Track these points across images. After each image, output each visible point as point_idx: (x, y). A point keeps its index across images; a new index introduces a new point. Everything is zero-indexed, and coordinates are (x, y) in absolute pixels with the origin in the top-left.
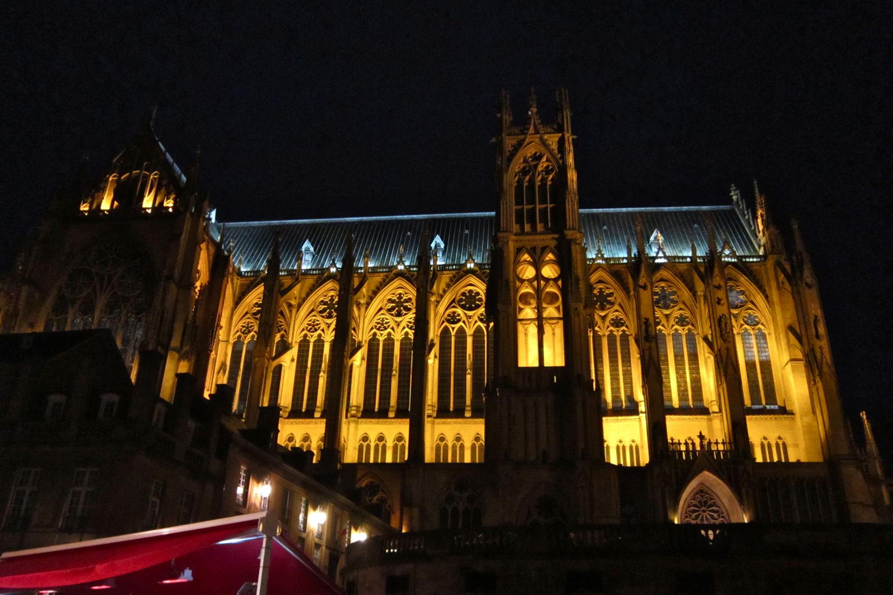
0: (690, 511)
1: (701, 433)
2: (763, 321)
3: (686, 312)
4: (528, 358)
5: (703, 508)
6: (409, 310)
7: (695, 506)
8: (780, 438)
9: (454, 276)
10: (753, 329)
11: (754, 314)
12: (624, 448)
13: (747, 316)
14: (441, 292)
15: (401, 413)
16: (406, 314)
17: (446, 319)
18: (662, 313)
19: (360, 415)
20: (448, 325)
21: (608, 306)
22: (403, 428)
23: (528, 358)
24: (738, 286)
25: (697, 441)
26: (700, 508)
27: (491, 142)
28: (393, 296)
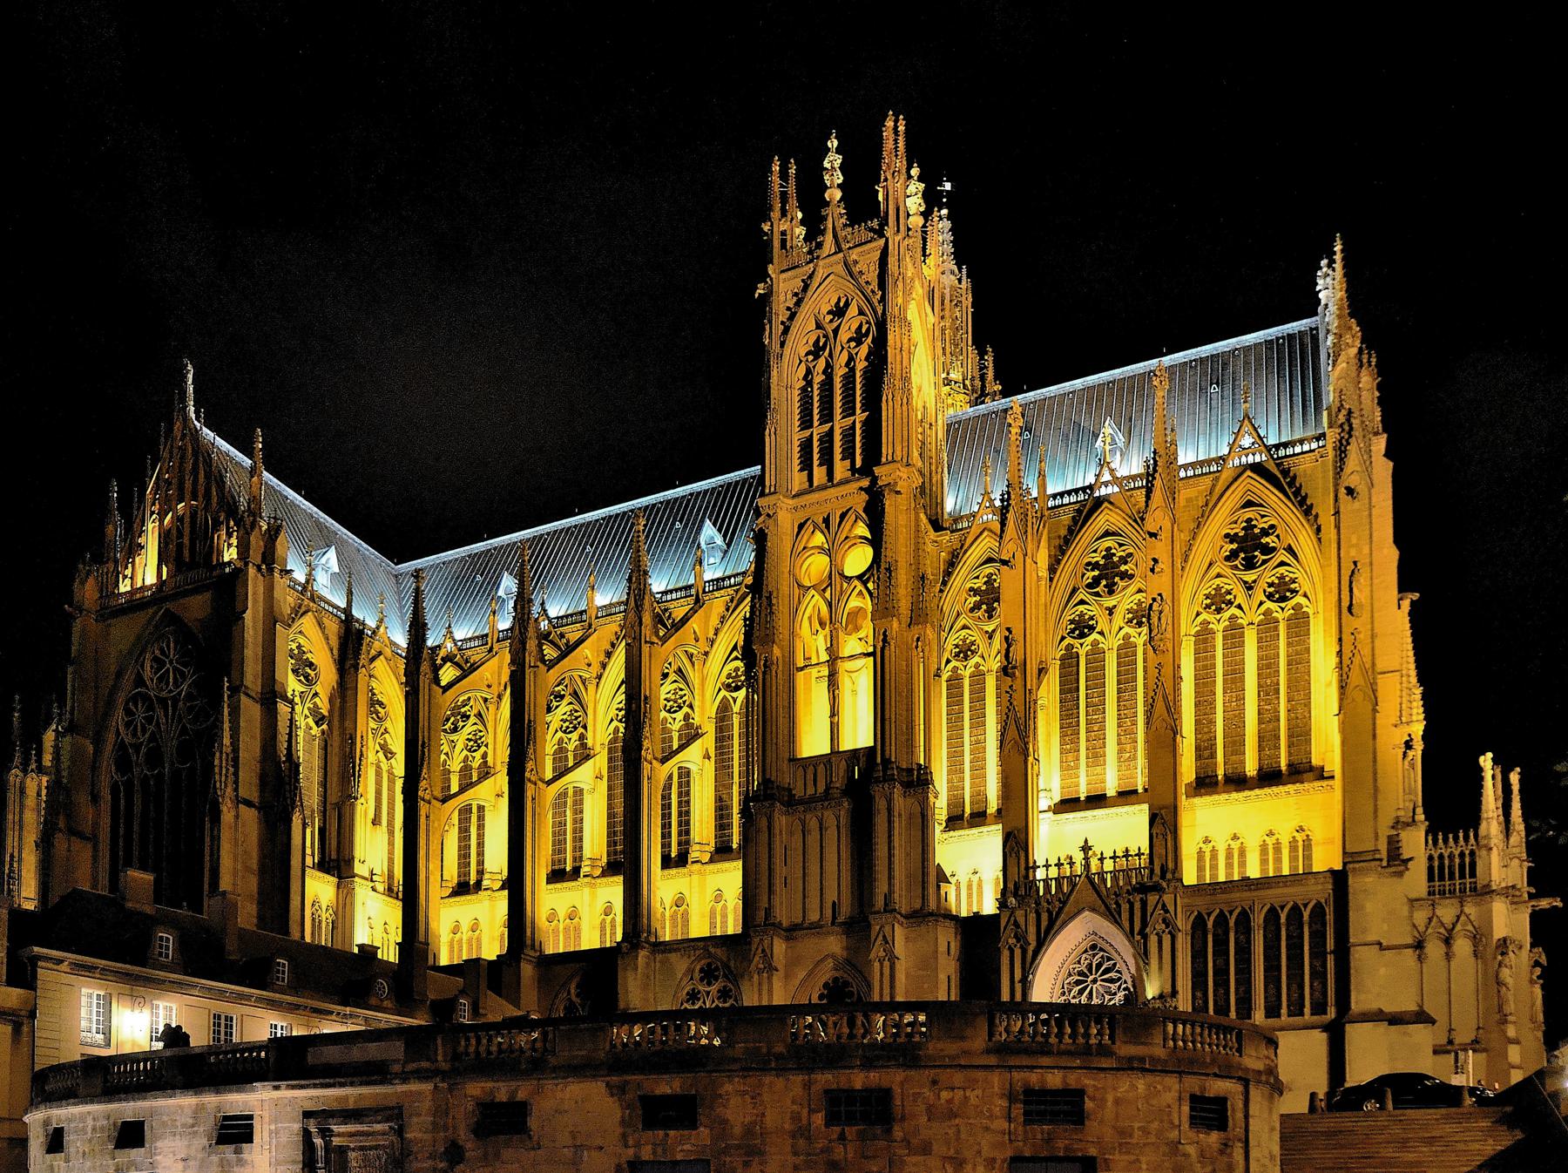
1: (1086, 841)
3: (1229, 582)
4: (813, 742)
6: (562, 697)
8: (1301, 829)
9: (732, 601)
12: (1277, 848)
14: (711, 635)
15: (611, 869)
17: (723, 684)
19: (598, 872)
20: (727, 694)
21: (1122, 584)
22: (613, 891)
23: (813, 742)
25: (1079, 857)
28: (976, 581)
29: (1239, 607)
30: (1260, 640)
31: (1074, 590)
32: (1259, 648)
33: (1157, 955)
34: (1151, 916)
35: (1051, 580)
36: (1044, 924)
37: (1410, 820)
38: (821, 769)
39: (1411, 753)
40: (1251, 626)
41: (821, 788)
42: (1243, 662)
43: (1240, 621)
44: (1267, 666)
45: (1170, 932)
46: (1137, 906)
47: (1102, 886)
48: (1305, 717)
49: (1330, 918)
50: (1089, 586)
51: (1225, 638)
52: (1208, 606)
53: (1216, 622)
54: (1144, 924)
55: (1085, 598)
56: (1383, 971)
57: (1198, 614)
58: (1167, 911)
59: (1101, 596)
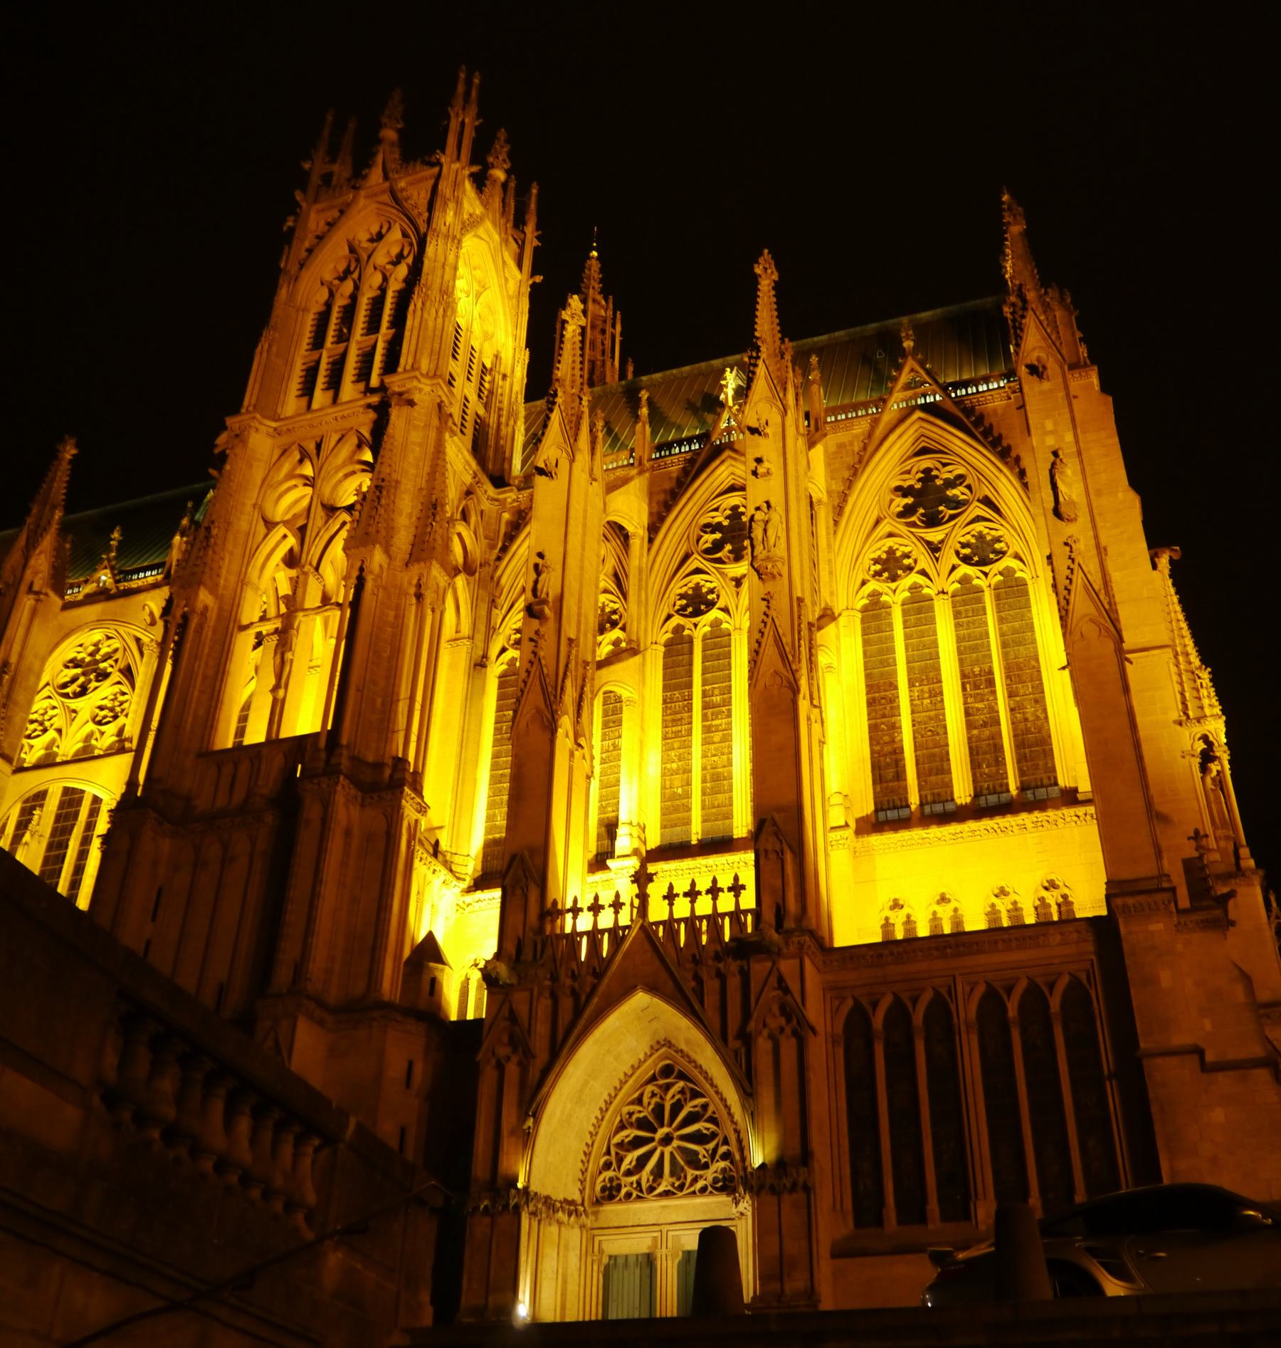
0: (620, 1145)
2: (1016, 546)
5: (662, 1132)
7: (642, 1124)
10: (986, 574)
11: (993, 533)
13: (973, 541)
16: (96, 688)
18: (723, 575)
24: (945, 465)
26: (655, 1131)
27: (285, 228)
29: (923, 573)
30: (957, 615)
31: (687, 557)
32: (958, 626)
33: (771, 1078)
34: (757, 1003)
35: (651, 541)
36: (565, 1015)
37: (1233, 869)
38: (244, 767)
39: (1214, 767)
40: (941, 596)
41: (239, 796)
42: (935, 644)
43: (926, 591)
44: (970, 648)
45: (795, 1033)
46: (734, 982)
47: (670, 946)
48: (1038, 718)
49: (1099, 1005)
50: (707, 551)
51: (905, 613)
52: (878, 574)
53: (891, 593)
54: (746, 1015)
55: (701, 566)
56: (1218, 1115)
57: (864, 583)
58: (786, 991)
59: (724, 563)
